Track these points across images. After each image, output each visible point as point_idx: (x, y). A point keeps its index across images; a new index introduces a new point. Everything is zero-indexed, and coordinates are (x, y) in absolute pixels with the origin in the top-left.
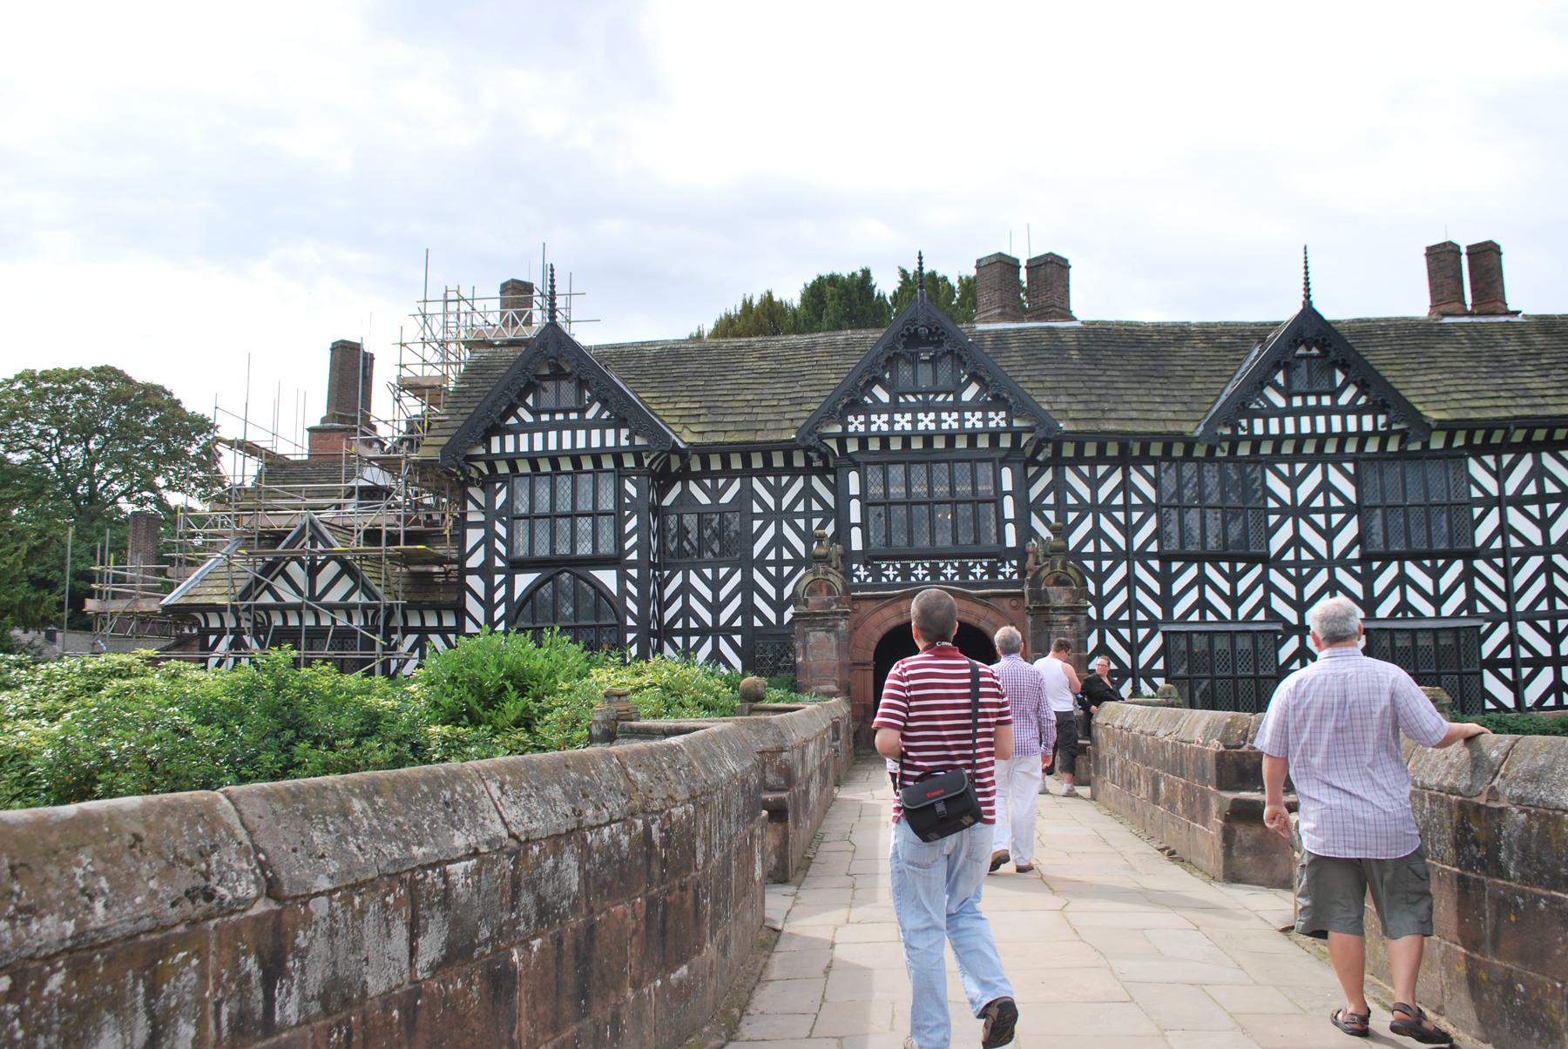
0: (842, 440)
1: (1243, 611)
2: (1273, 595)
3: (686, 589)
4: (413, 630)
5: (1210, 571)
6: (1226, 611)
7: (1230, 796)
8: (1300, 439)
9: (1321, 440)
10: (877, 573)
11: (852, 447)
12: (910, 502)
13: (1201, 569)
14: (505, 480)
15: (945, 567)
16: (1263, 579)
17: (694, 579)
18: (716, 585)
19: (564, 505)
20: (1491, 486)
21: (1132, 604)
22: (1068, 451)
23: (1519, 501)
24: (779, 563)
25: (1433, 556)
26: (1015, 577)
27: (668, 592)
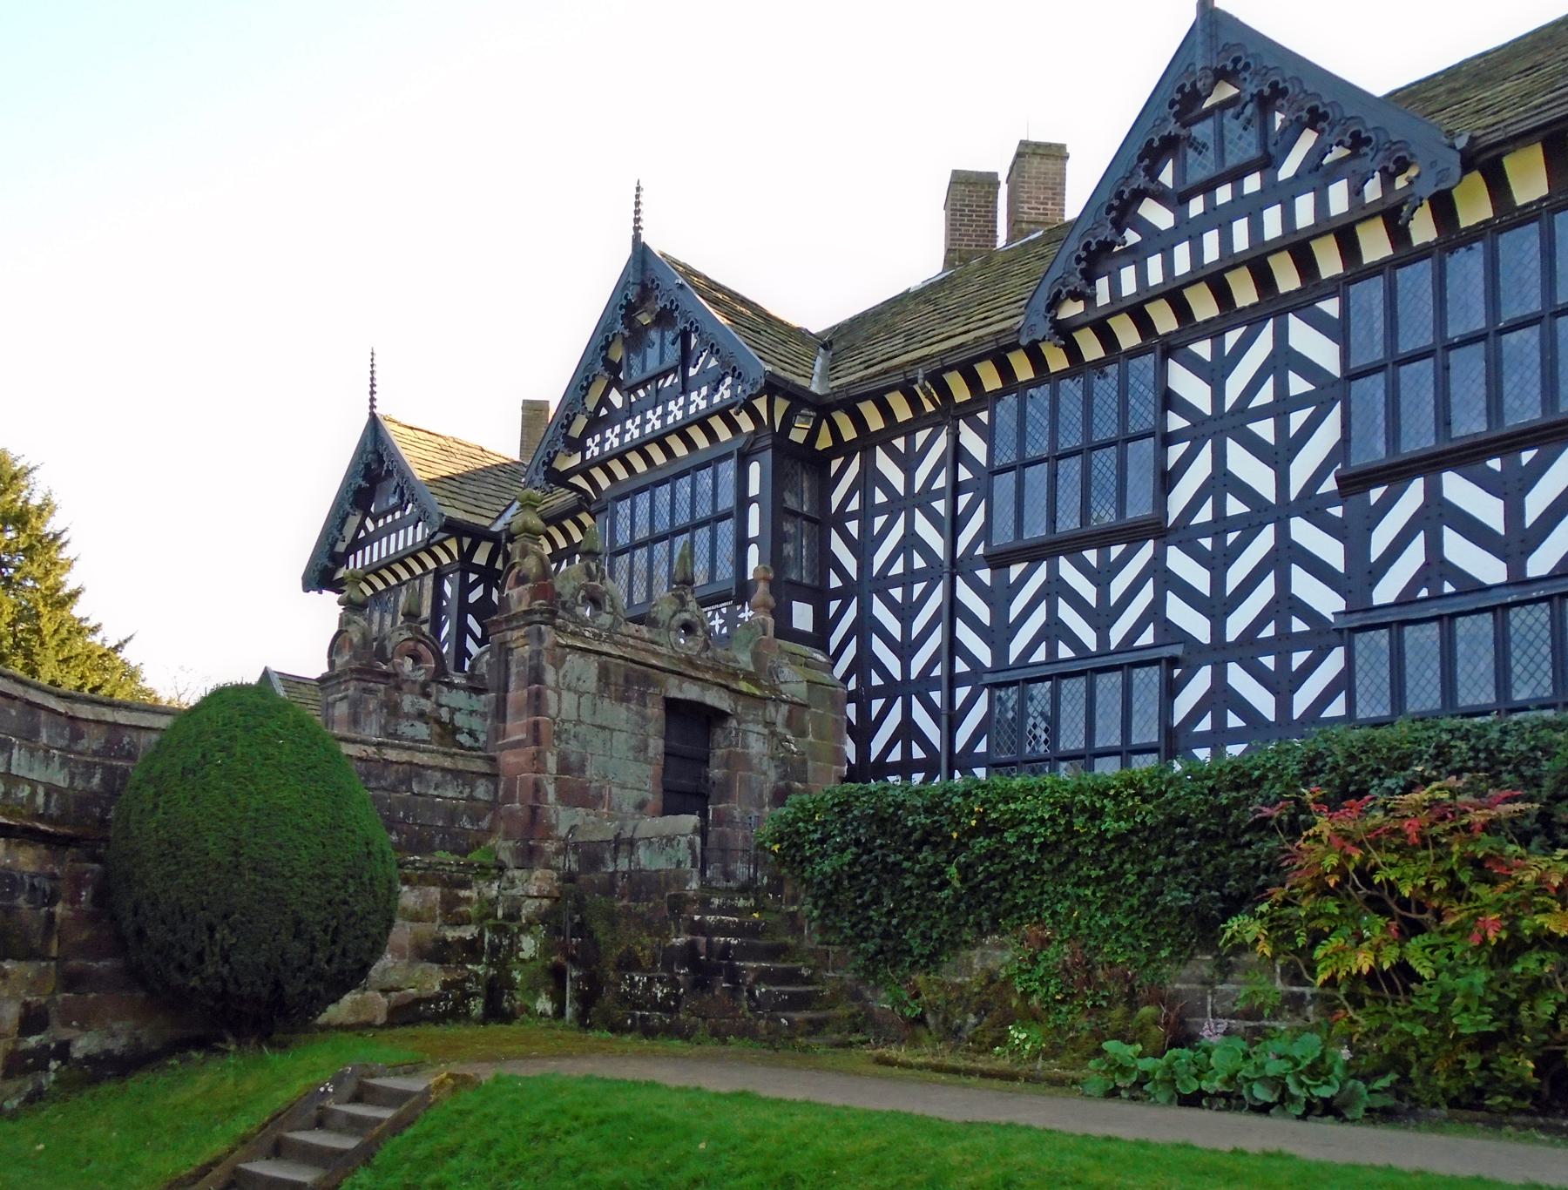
1: (1117, 634)
2: (1171, 597)
5: (1067, 570)
13: (1053, 572)
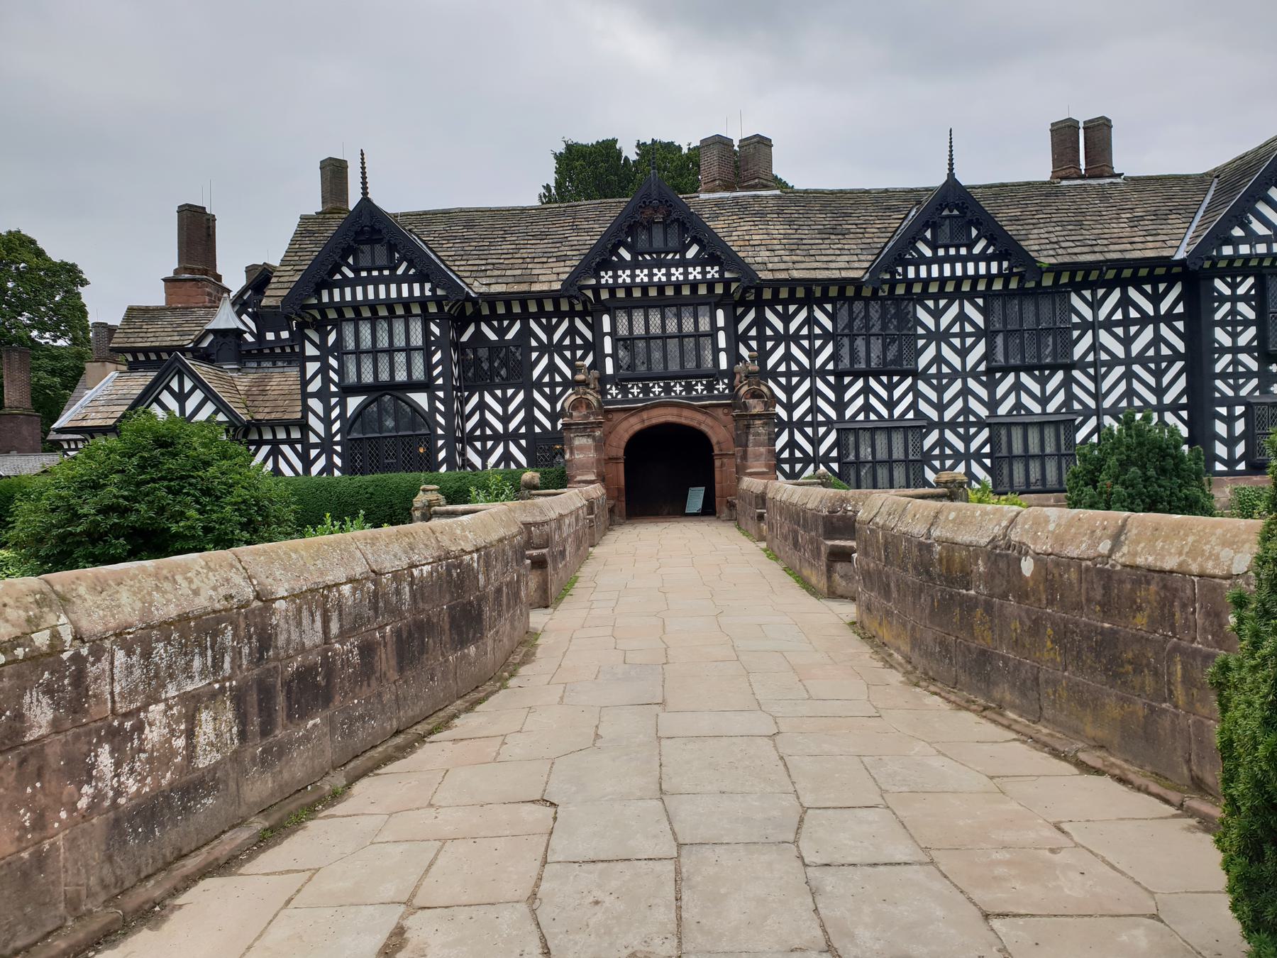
0: (596, 289)
1: (897, 412)
3: (482, 406)
4: (267, 442)
5: (873, 383)
6: (884, 412)
7: (830, 543)
8: (942, 280)
9: (959, 281)
10: (625, 391)
11: (605, 295)
12: (648, 338)
13: (866, 382)
14: (337, 325)
16: (913, 388)
17: (488, 399)
18: (505, 402)
19: (383, 342)
20: (1087, 313)
21: (814, 409)
22: (767, 294)
23: (1108, 325)
24: (552, 384)
25: (1042, 368)
27: (468, 408)
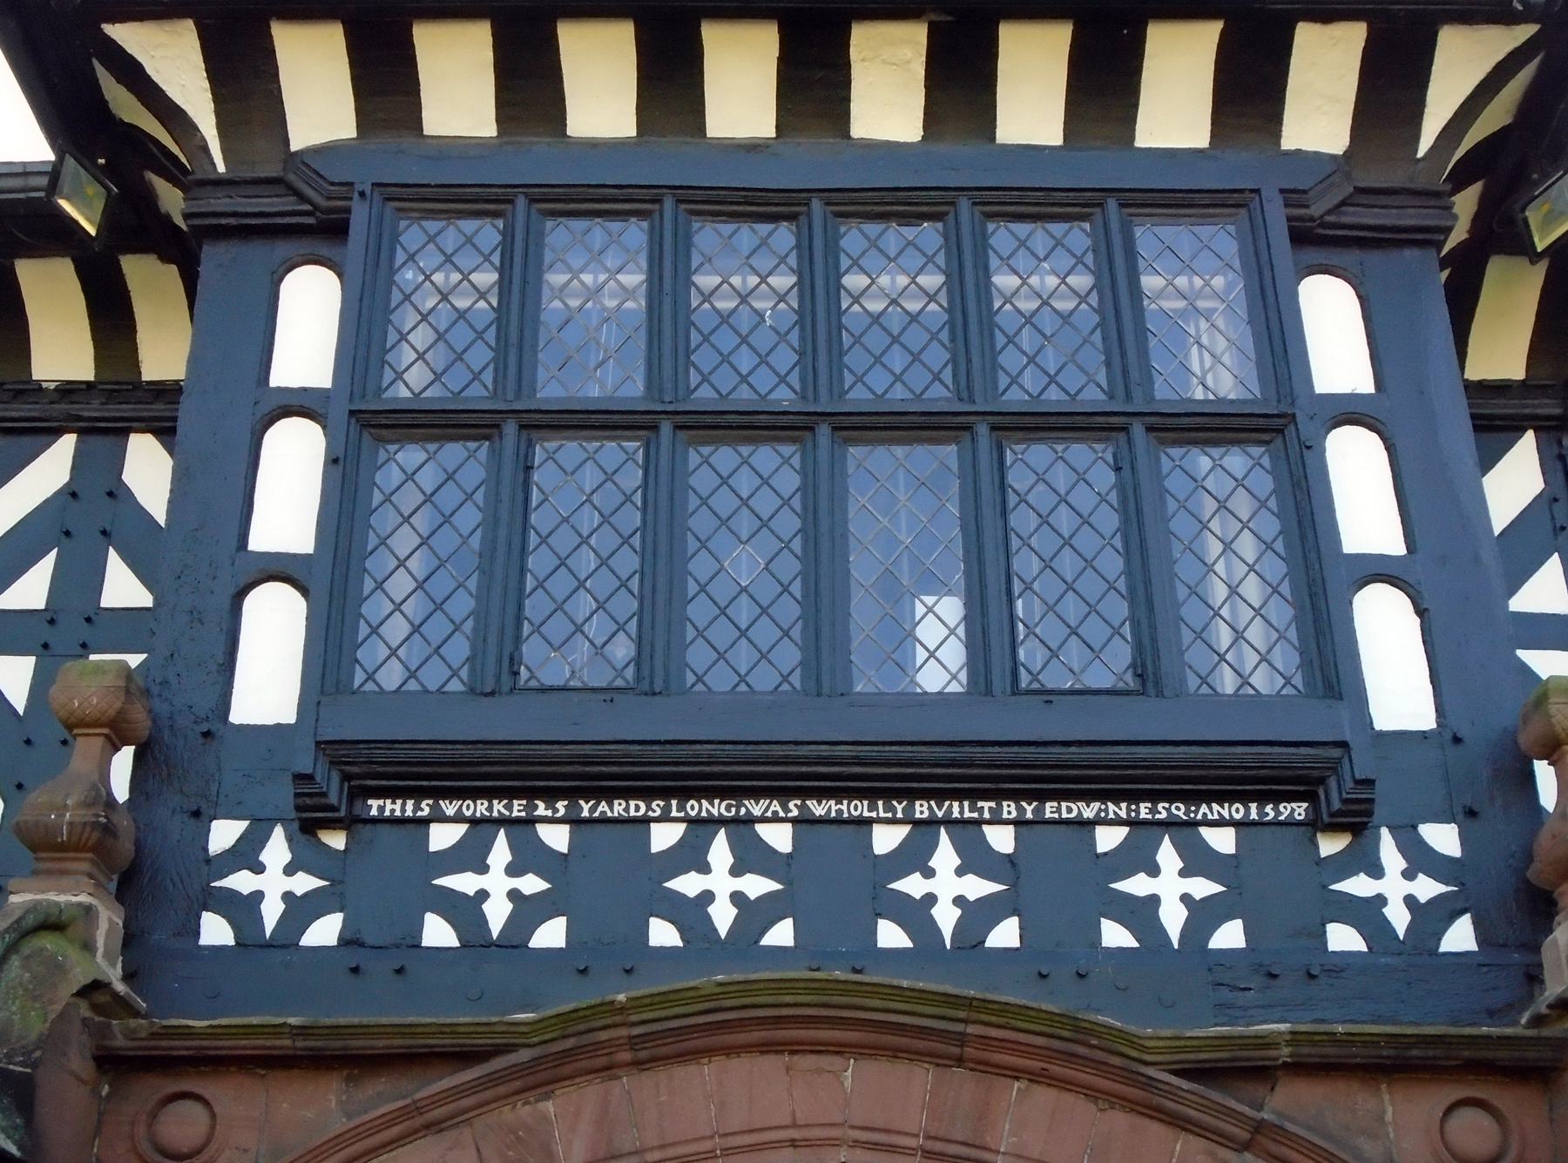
12: (669, 423)
15: (915, 857)
26: (1460, 937)
